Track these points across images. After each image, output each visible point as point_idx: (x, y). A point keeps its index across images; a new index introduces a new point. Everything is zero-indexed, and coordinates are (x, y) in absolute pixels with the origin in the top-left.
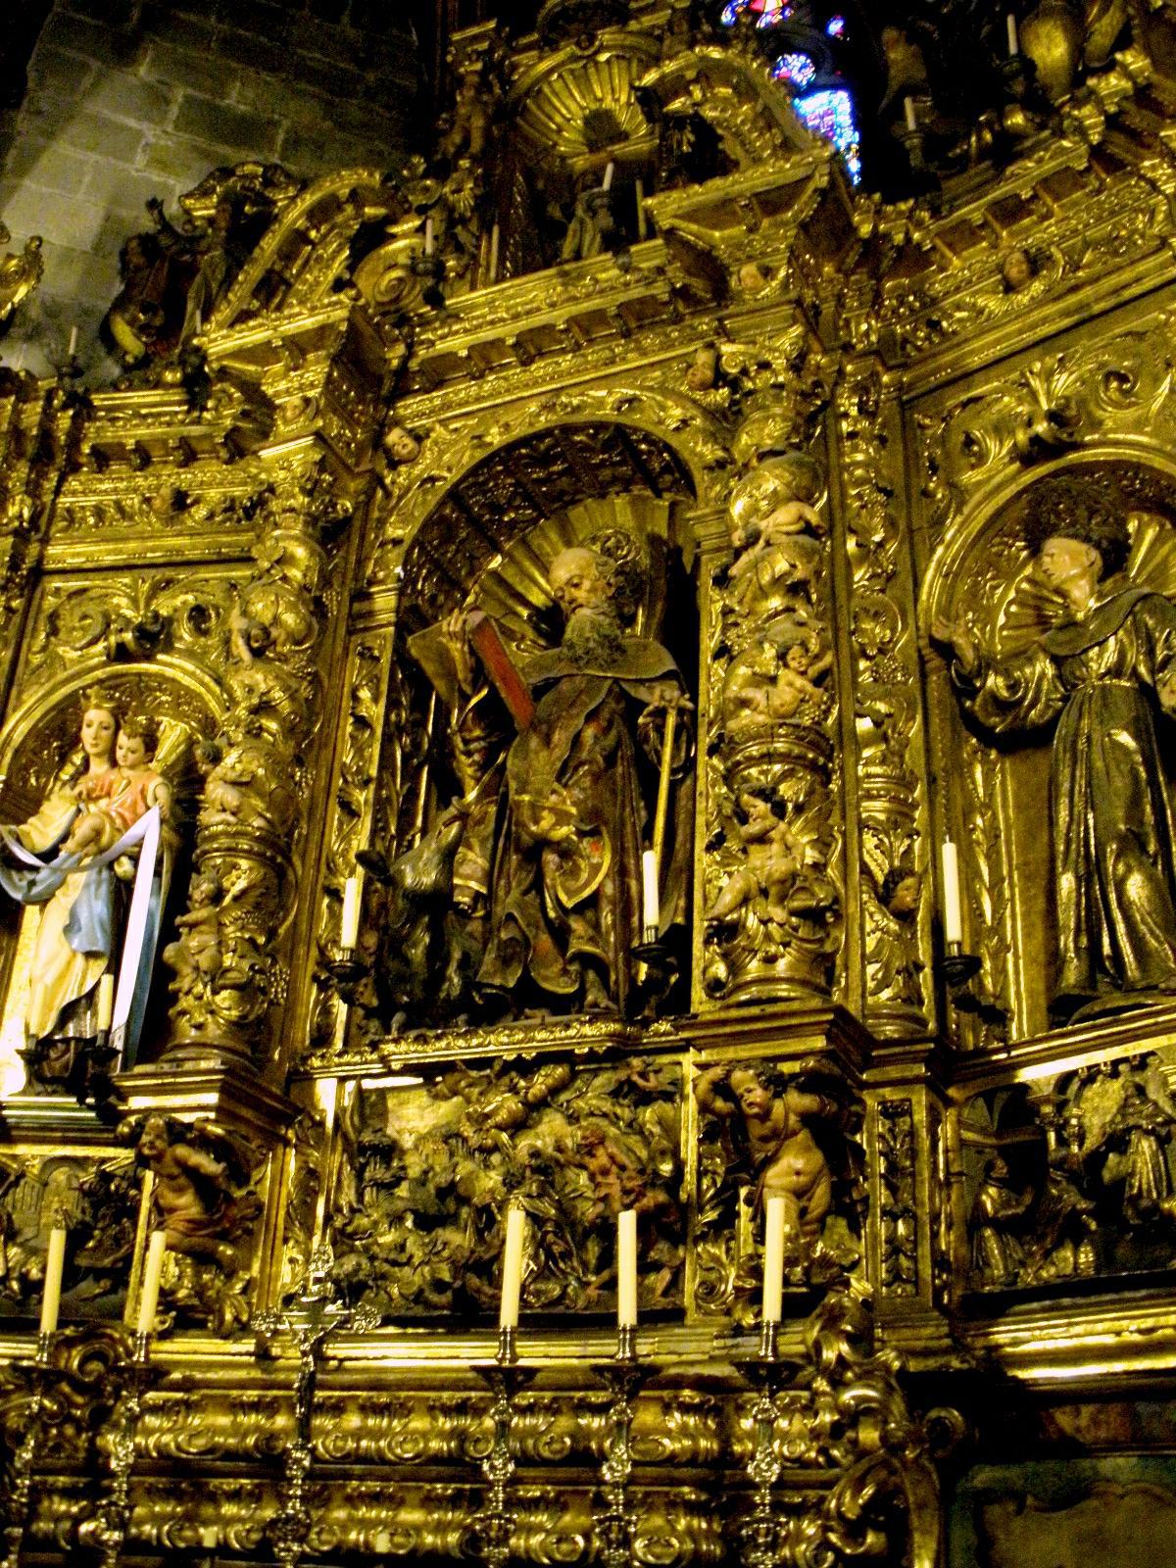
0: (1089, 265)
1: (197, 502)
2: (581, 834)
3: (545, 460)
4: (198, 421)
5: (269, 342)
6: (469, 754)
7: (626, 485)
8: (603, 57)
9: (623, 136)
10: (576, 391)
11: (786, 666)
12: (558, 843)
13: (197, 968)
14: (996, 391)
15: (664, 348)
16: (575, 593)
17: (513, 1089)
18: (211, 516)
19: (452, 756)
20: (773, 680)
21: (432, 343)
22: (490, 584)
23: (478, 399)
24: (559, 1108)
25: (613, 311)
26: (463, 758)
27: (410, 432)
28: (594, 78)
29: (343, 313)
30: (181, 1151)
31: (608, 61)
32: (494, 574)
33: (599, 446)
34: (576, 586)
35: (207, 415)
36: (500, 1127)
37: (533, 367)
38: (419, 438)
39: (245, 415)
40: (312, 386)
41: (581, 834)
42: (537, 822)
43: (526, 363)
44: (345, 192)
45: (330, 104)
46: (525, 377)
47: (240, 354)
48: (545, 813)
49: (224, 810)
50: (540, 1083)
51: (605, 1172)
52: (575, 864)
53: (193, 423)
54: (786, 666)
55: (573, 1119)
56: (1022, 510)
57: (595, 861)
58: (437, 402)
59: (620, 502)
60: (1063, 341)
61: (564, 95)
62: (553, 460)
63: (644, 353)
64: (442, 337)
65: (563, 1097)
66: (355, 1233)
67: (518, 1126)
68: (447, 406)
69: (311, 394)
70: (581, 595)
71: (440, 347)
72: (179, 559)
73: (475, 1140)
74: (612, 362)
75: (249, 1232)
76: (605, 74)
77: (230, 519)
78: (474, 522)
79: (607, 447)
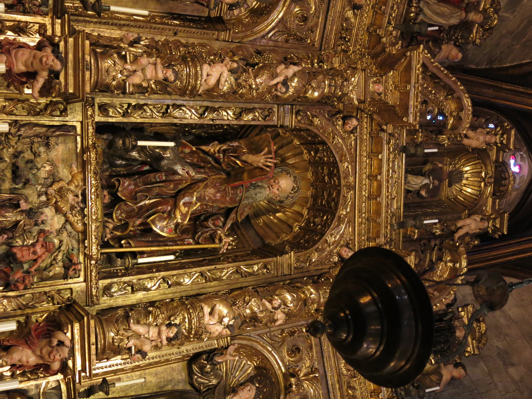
0: (347, 391)
1: (354, 14)
2: (177, 225)
3: (331, 175)
4: (389, 23)
5: (410, 83)
6: (219, 151)
7: (315, 197)
8: (483, 184)
9: (450, 185)
10: (353, 196)
11: (224, 328)
12: (174, 213)
13: (135, 71)
14: (313, 356)
15: (359, 234)
16: (276, 189)
17: (72, 208)
18: (347, 19)
19: (221, 142)
20: (221, 321)
21: (388, 143)
22: (290, 139)
23: (361, 155)
24: (64, 227)
25: (378, 220)
26: (218, 148)
27: (355, 128)
28: (476, 179)
29: (411, 120)
30: (45, 74)
31: (480, 187)
32: (292, 141)
33: (330, 200)
34: (278, 189)
35: (391, 28)
36: (56, 202)
37: (367, 180)
38: (352, 132)
39: (384, 50)
40: (385, 95)
41: (177, 225)
42: (185, 204)
43: (369, 177)
44: (462, 114)
45: (513, 33)
46: (364, 176)
47: (409, 68)
48: (186, 209)
49: (208, 75)
50: (75, 219)
51: (35, 253)
52: (165, 219)
53: (389, 19)
54: (224, 328)
55: (59, 232)
56: (268, 366)
57: (165, 229)
58: (365, 137)
59: (309, 193)
60: (324, 381)
61: (474, 166)
62: (330, 178)
63: (360, 224)
64: (389, 149)
65: (68, 227)
66: (8, 138)
67: (58, 210)
68: (362, 140)
69: (383, 95)
70: (275, 190)
71: (385, 147)
72: (331, 4)
73: (51, 191)
74: (360, 211)
75: (8, 86)
76: (476, 184)
77: (343, 29)
78: (314, 143)
79: (328, 202)
